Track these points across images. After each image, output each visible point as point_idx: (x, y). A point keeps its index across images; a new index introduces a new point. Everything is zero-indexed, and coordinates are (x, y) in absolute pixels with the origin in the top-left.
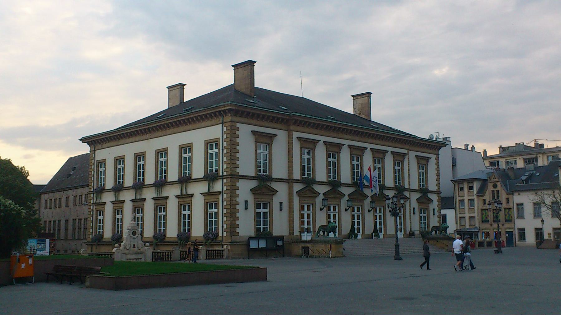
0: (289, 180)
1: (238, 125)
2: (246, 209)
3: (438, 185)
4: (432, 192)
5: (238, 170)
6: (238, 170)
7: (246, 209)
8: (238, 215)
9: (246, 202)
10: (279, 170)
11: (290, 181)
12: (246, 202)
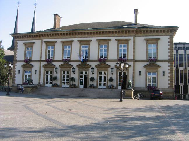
0: (41, 60)
1: (18, 42)
2: (19, 73)
3: (134, 56)
4: (130, 60)
5: (16, 59)
6: (16, 59)
7: (19, 73)
8: (15, 75)
9: (19, 71)
10: (36, 57)
11: (40, 61)
12: (19, 71)
